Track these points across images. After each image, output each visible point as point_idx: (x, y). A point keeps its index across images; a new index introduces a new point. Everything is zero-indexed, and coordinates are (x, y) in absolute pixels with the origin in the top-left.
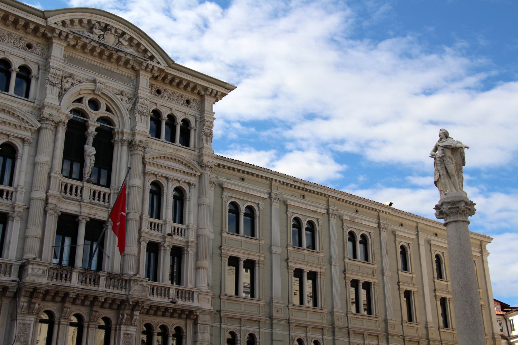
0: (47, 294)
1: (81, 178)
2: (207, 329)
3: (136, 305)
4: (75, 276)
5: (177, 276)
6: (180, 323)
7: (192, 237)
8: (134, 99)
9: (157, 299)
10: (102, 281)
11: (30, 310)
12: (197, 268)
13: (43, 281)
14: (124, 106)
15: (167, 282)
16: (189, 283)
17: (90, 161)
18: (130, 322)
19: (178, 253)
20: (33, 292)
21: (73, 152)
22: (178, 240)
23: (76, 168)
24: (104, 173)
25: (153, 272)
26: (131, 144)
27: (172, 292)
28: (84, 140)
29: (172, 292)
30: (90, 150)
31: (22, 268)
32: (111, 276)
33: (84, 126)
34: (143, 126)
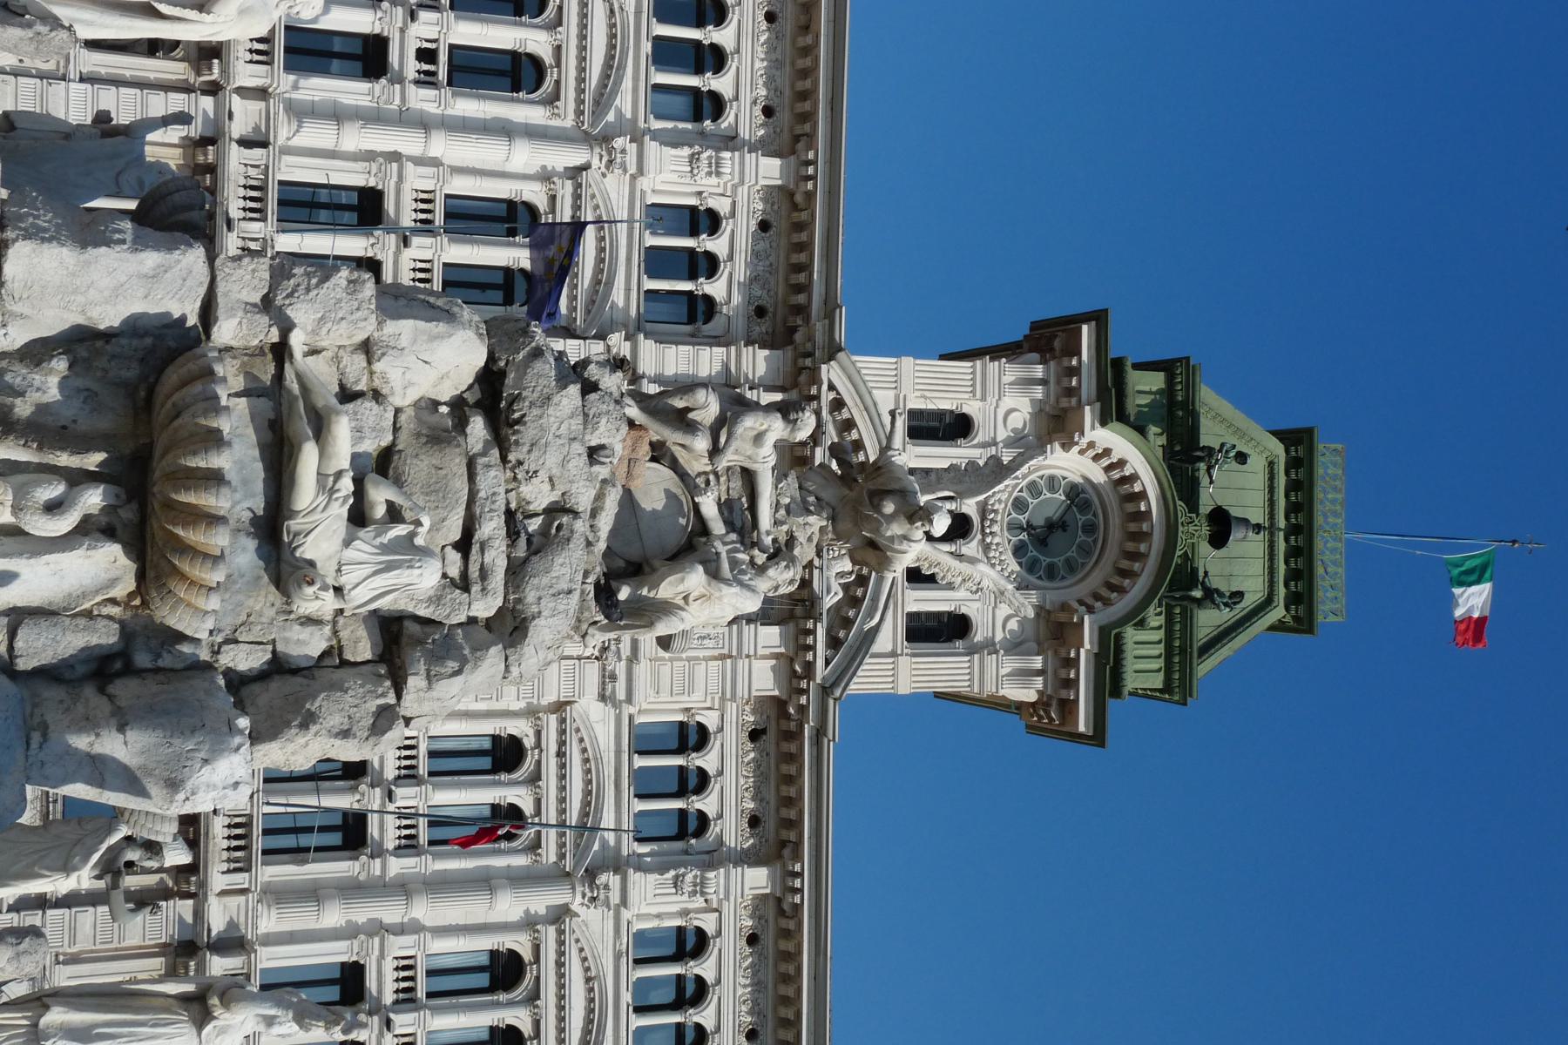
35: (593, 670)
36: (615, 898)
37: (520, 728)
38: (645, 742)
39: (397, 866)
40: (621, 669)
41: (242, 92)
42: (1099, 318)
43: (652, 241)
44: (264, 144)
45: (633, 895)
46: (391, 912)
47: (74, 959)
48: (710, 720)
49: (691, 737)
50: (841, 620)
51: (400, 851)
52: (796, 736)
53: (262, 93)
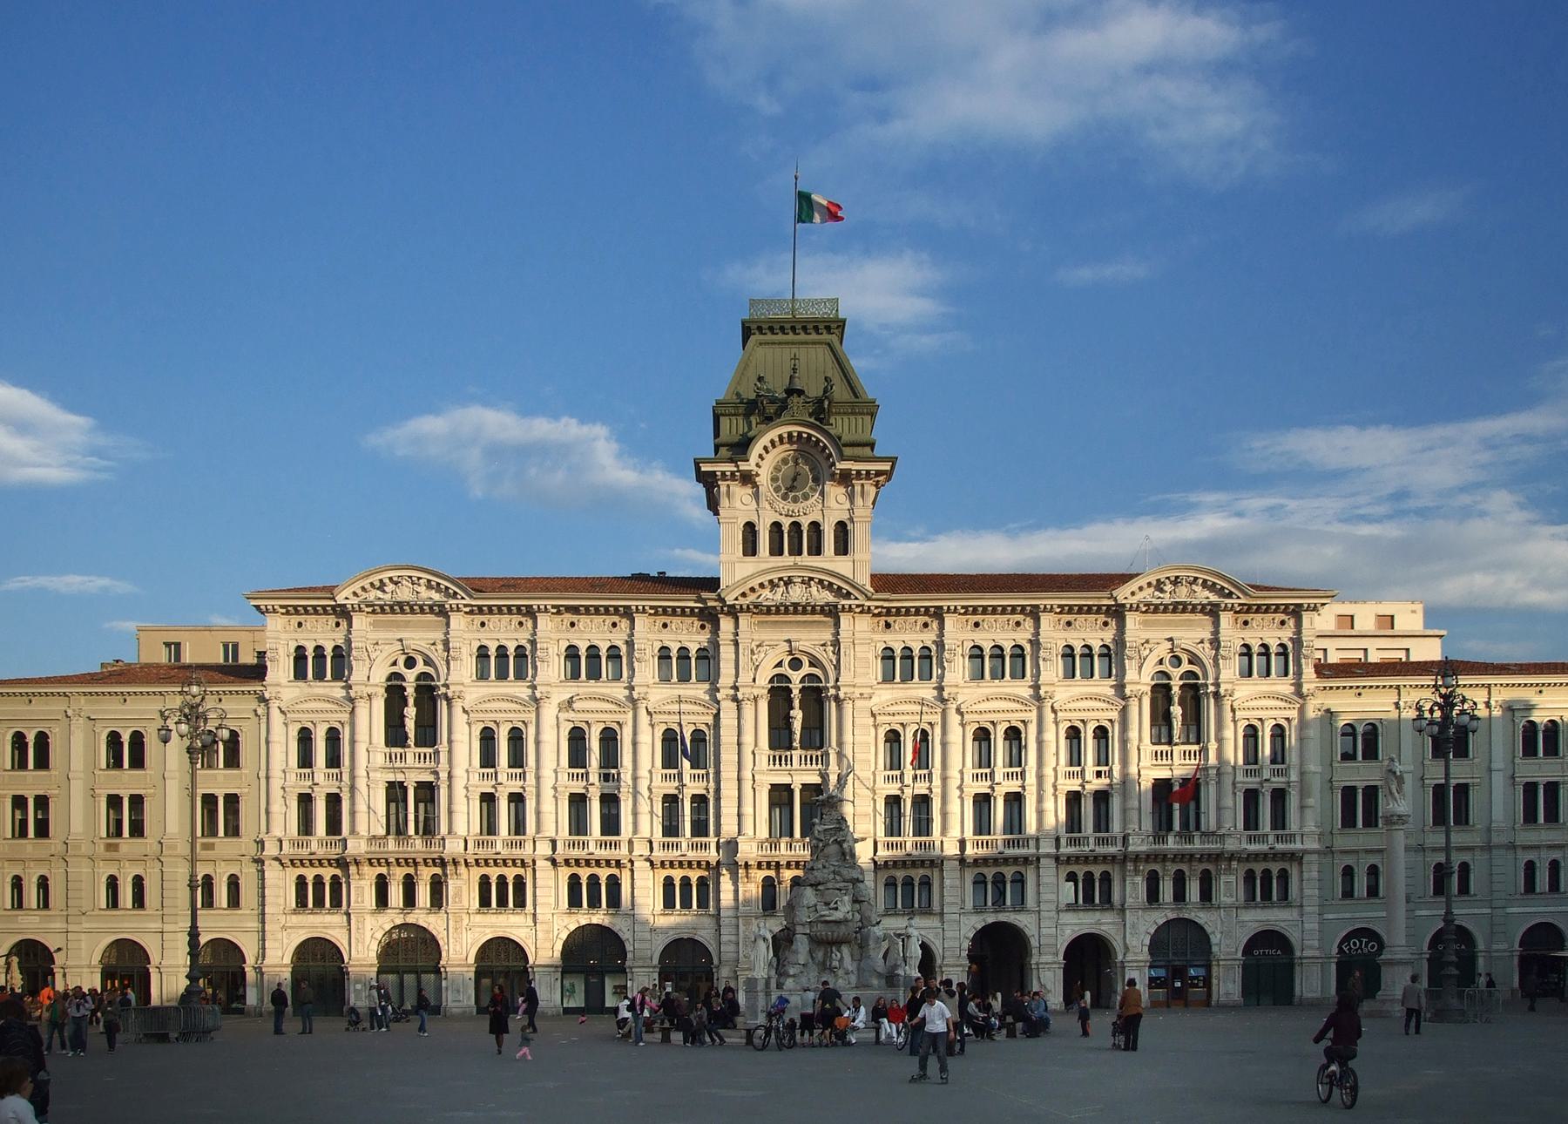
0: (1150, 857)
1: (1170, 742)
2: (1315, 868)
3: (1232, 856)
4: (1171, 839)
5: (1279, 820)
6: (1286, 865)
7: (1294, 777)
8: (1215, 643)
9: (1253, 847)
10: (1197, 840)
11: (1137, 872)
12: (1302, 808)
13: (1144, 848)
14: (1206, 653)
15: (1268, 829)
16: (1293, 824)
17: (1177, 724)
18: (1229, 870)
19: (1279, 796)
20: (1137, 858)
21: (1161, 718)
22: (1278, 782)
23: (1164, 730)
24: (1193, 728)
25: (1251, 821)
26: (1217, 695)
27: (1271, 839)
28: (1169, 701)
29: (1271, 839)
30: (1176, 710)
31: (1125, 839)
32: (1204, 834)
33: (1168, 688)
34: (1230, 671)
35: (858, 703)
36: (954, 690)
37: (882, 732)
38: (888, 678)
39: (937, 782)
40: (858, 691)
41: (631, 851)
42: (697, 464)
43: (675, 679)
44: (651, 842)
45: (953, 682)
46: (954, 783)
47: (963, 901)
48: (881, 646)
49: (888, 656)
50: (839, 592)
51: (930, 781)
52: (889, 609)
53: (630, 842)
